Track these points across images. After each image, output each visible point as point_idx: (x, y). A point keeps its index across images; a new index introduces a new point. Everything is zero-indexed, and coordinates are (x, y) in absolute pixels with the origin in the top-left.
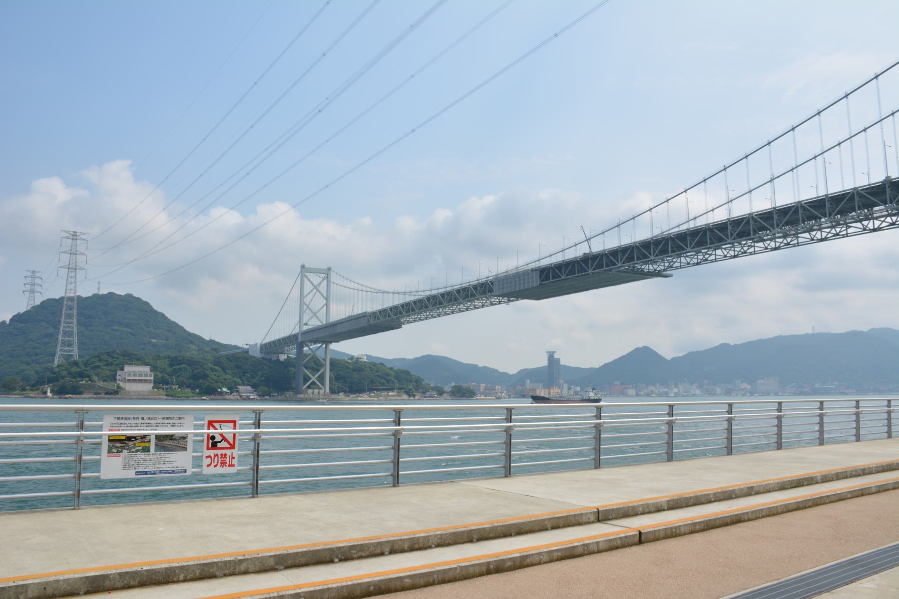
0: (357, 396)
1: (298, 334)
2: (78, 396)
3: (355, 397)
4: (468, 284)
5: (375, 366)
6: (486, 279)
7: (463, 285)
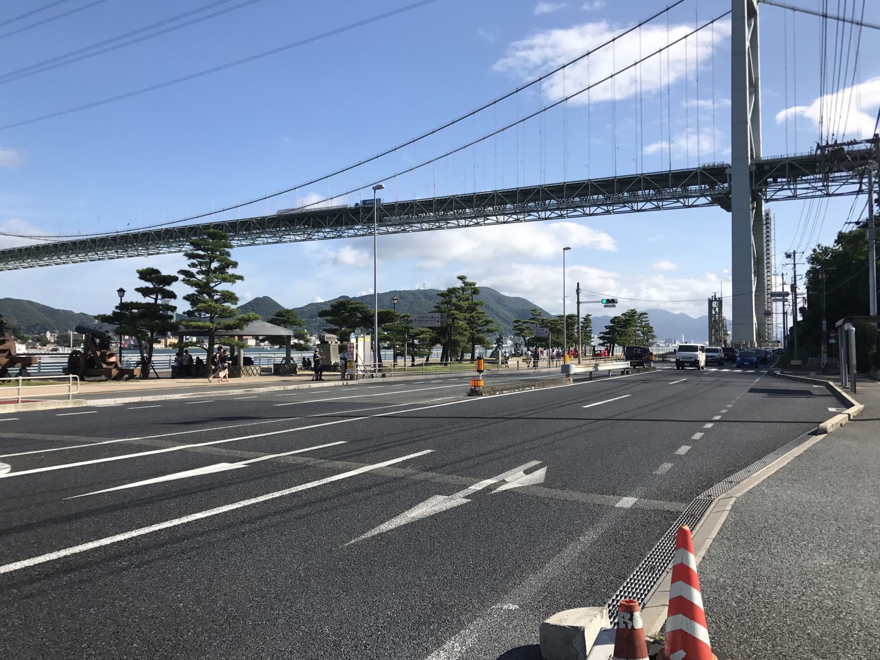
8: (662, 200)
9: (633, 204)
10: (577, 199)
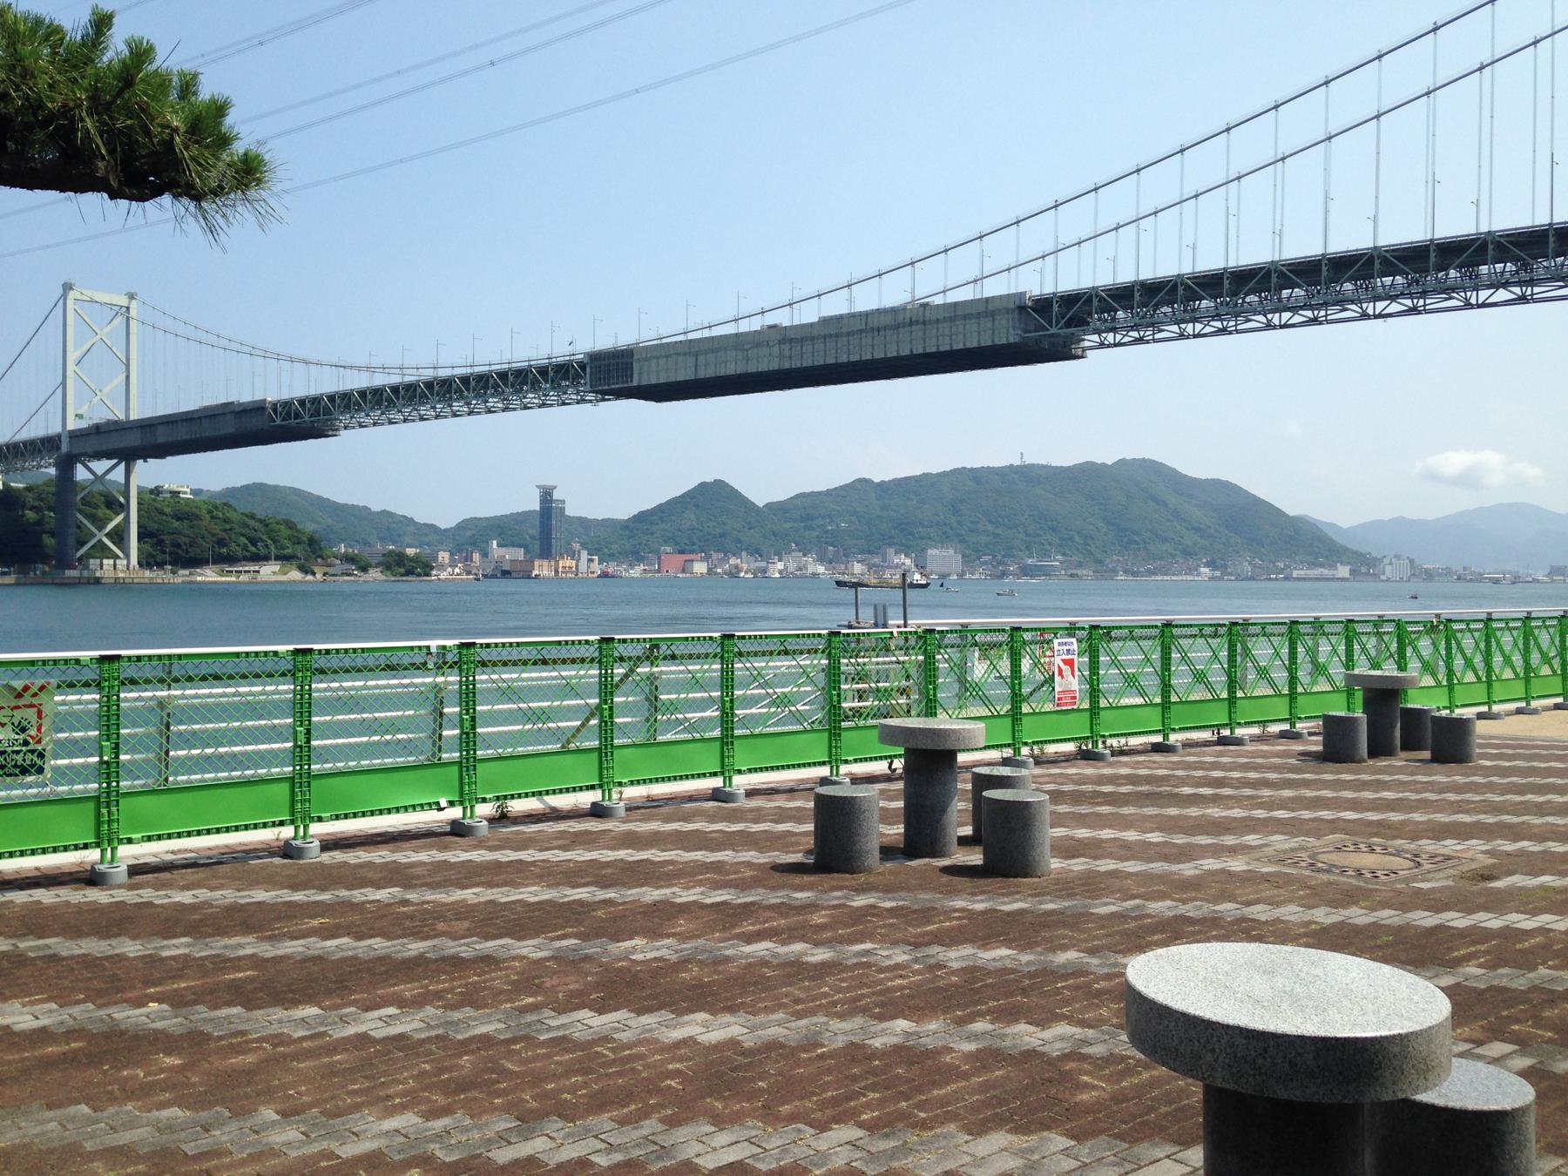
0: (191, 574)
1: (59, 436)
3: (186, 576)
4: (527, 364)
5: (216, 508)
6: (568, 358)
7: (514, 365)
8: (1532, 283)
9: (1469, 294)
10: (1348, 286)
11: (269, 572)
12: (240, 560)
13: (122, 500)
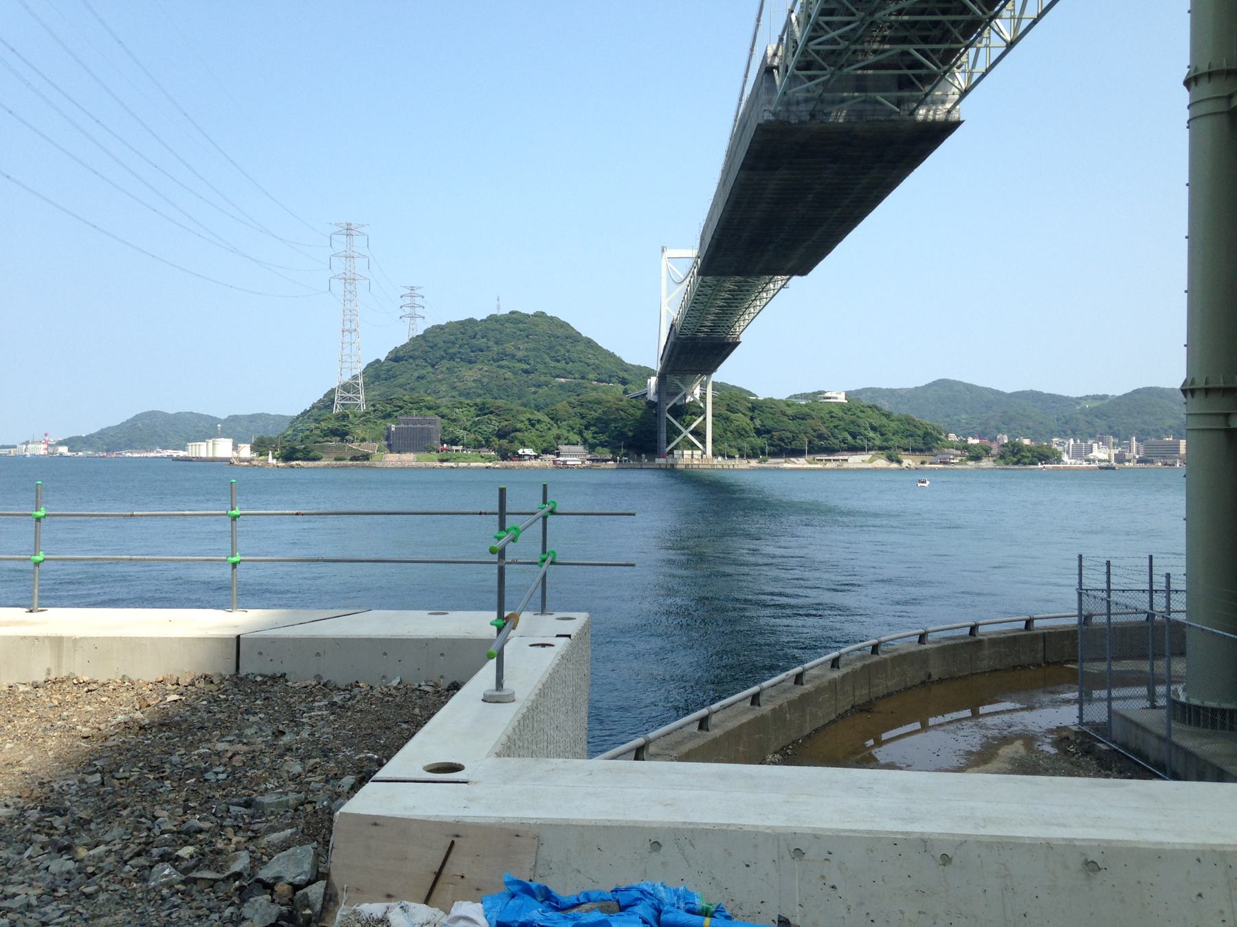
2: (311, 464)
11: (855, 460)
12: (839, 451)
13: (702, 405)
